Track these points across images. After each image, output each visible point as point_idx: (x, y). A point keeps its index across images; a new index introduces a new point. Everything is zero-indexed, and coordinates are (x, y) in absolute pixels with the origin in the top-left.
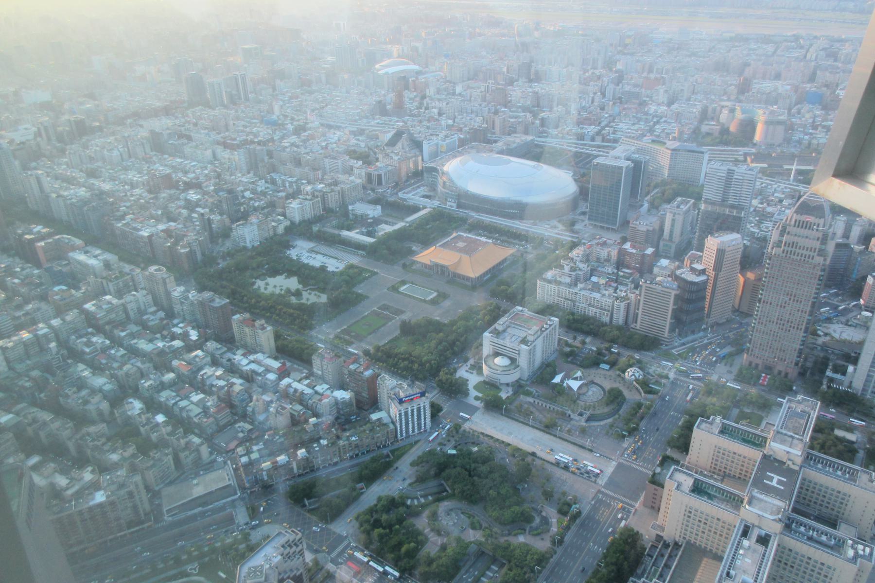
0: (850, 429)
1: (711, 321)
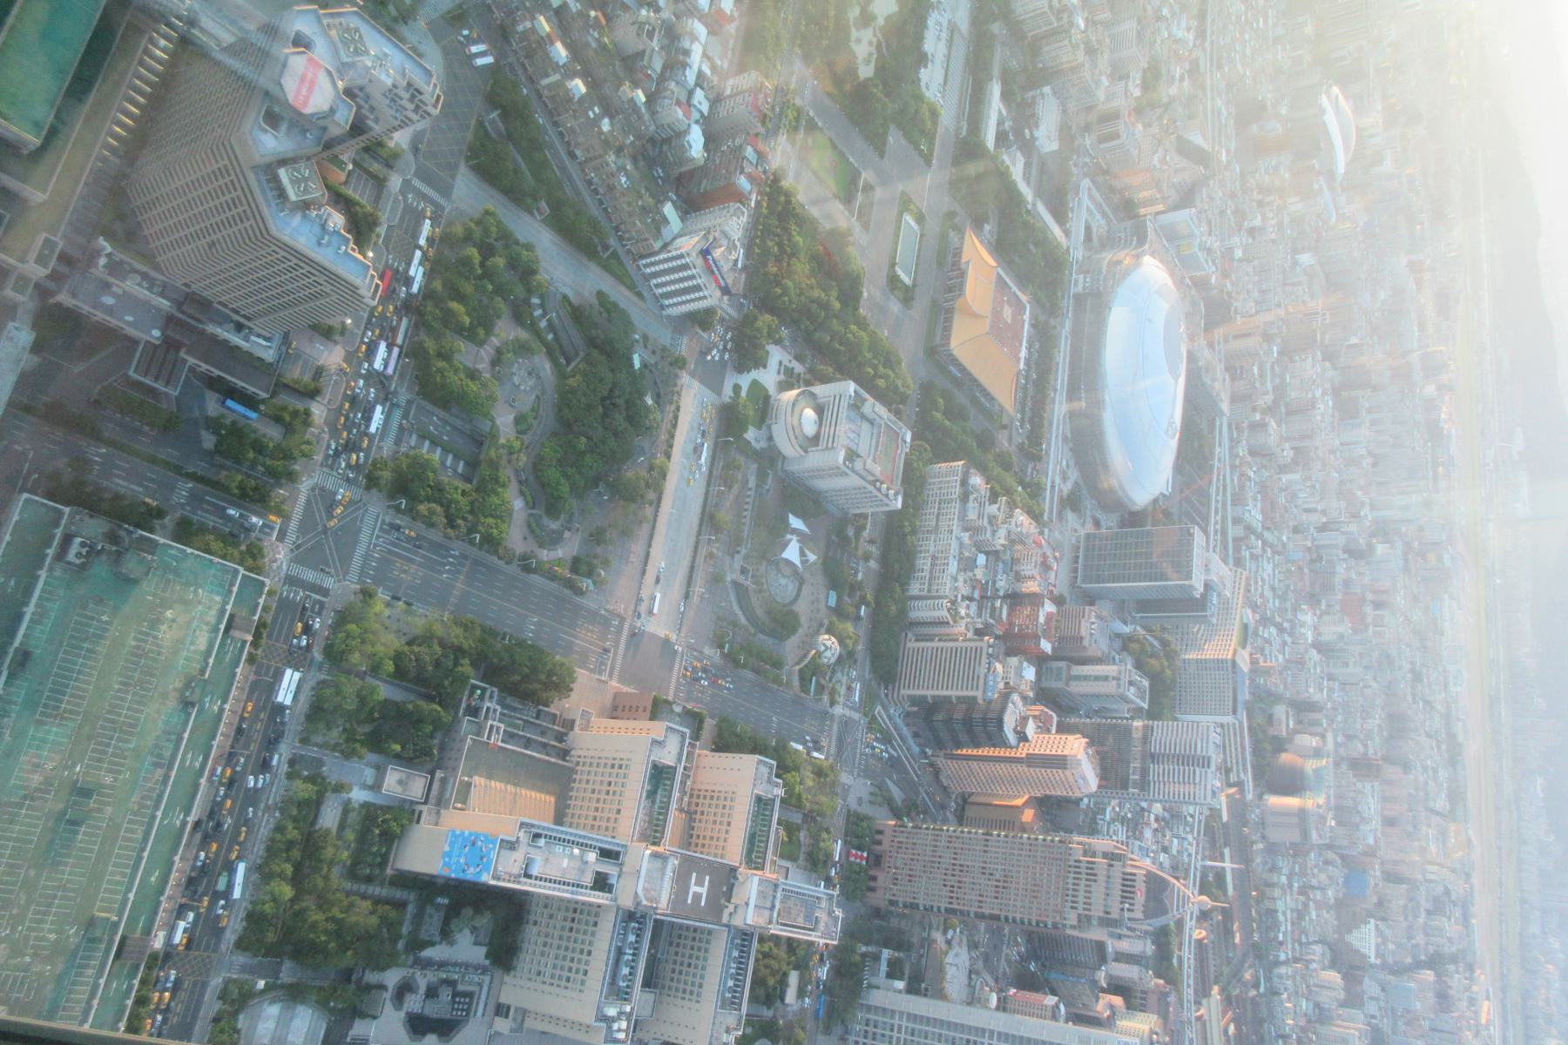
0: (801, 993)
1: (941, 761)
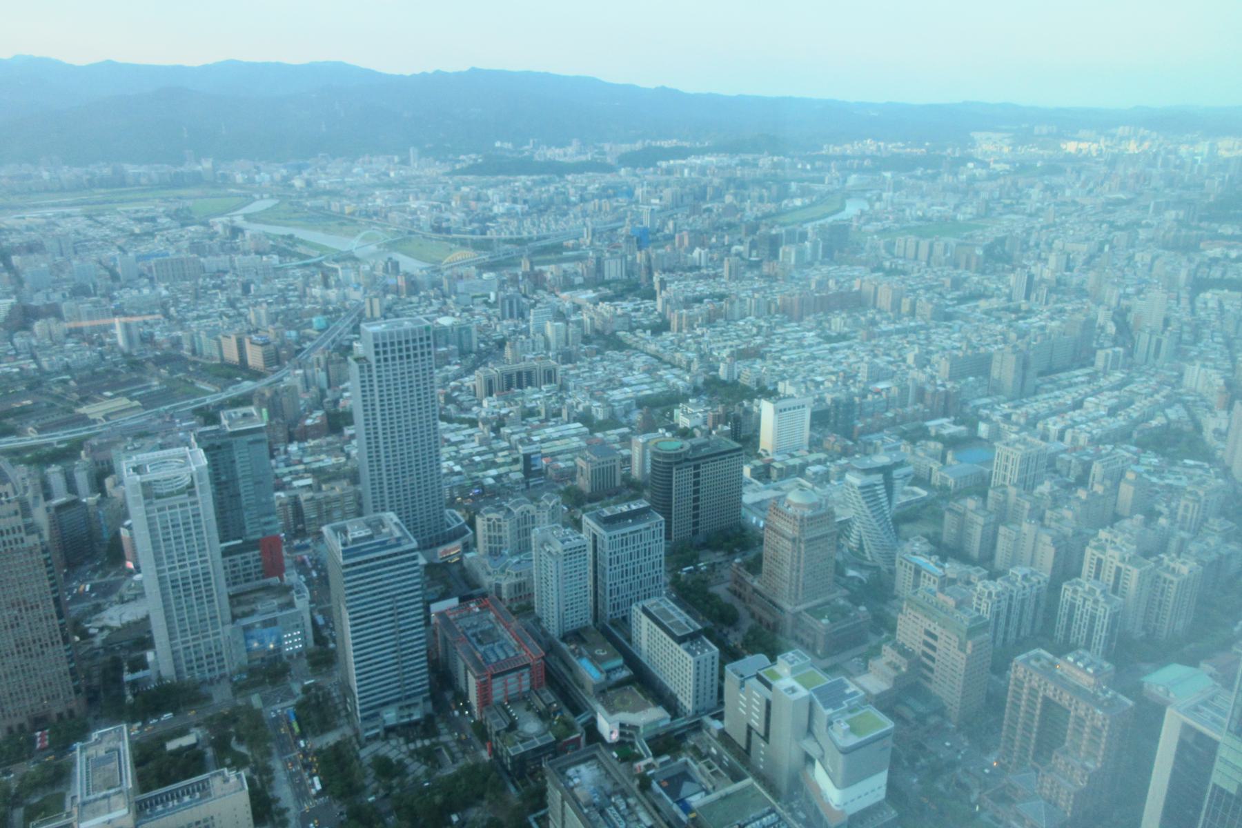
0: (183, 732)
